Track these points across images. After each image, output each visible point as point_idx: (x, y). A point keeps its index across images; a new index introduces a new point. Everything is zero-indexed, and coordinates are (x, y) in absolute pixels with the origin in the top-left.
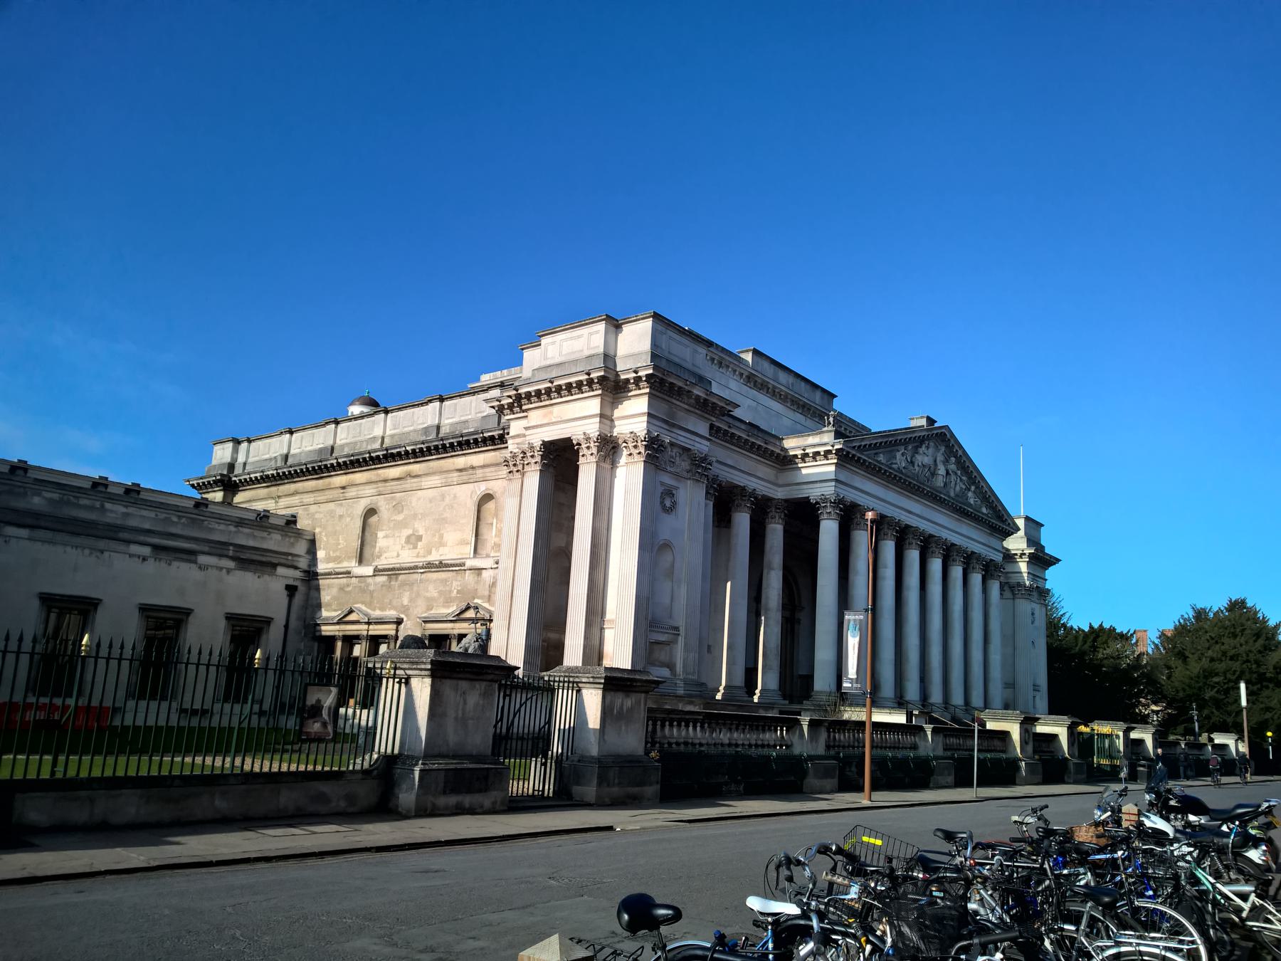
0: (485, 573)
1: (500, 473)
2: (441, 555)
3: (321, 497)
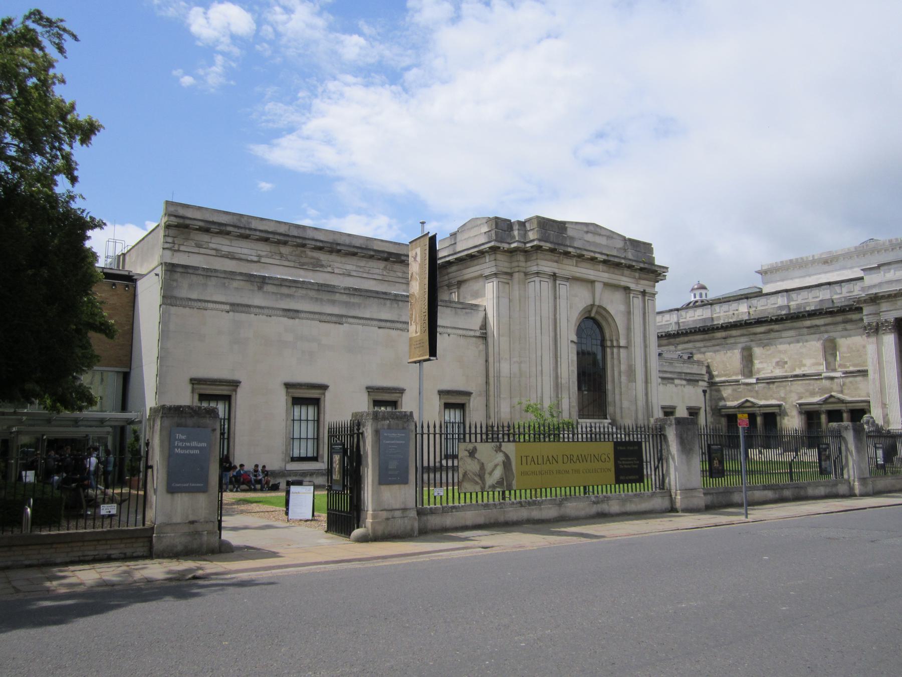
3: (708, 344)
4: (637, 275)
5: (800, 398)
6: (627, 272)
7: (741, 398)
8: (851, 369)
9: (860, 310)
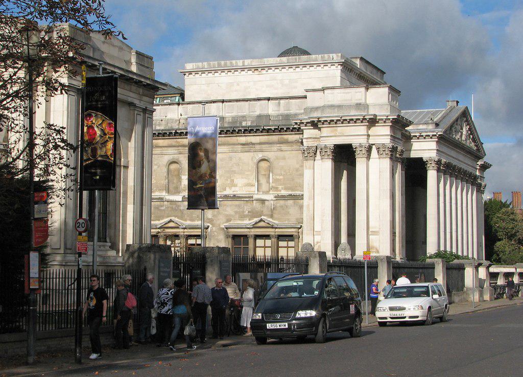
0: (267, 203)
1: (272, 148)
2: (233, 191)
4: (141, 91)
5: (229, 220)
6: (134, 88)
7: (163, 218)
8: (284, 193)
9: (299, 130)
